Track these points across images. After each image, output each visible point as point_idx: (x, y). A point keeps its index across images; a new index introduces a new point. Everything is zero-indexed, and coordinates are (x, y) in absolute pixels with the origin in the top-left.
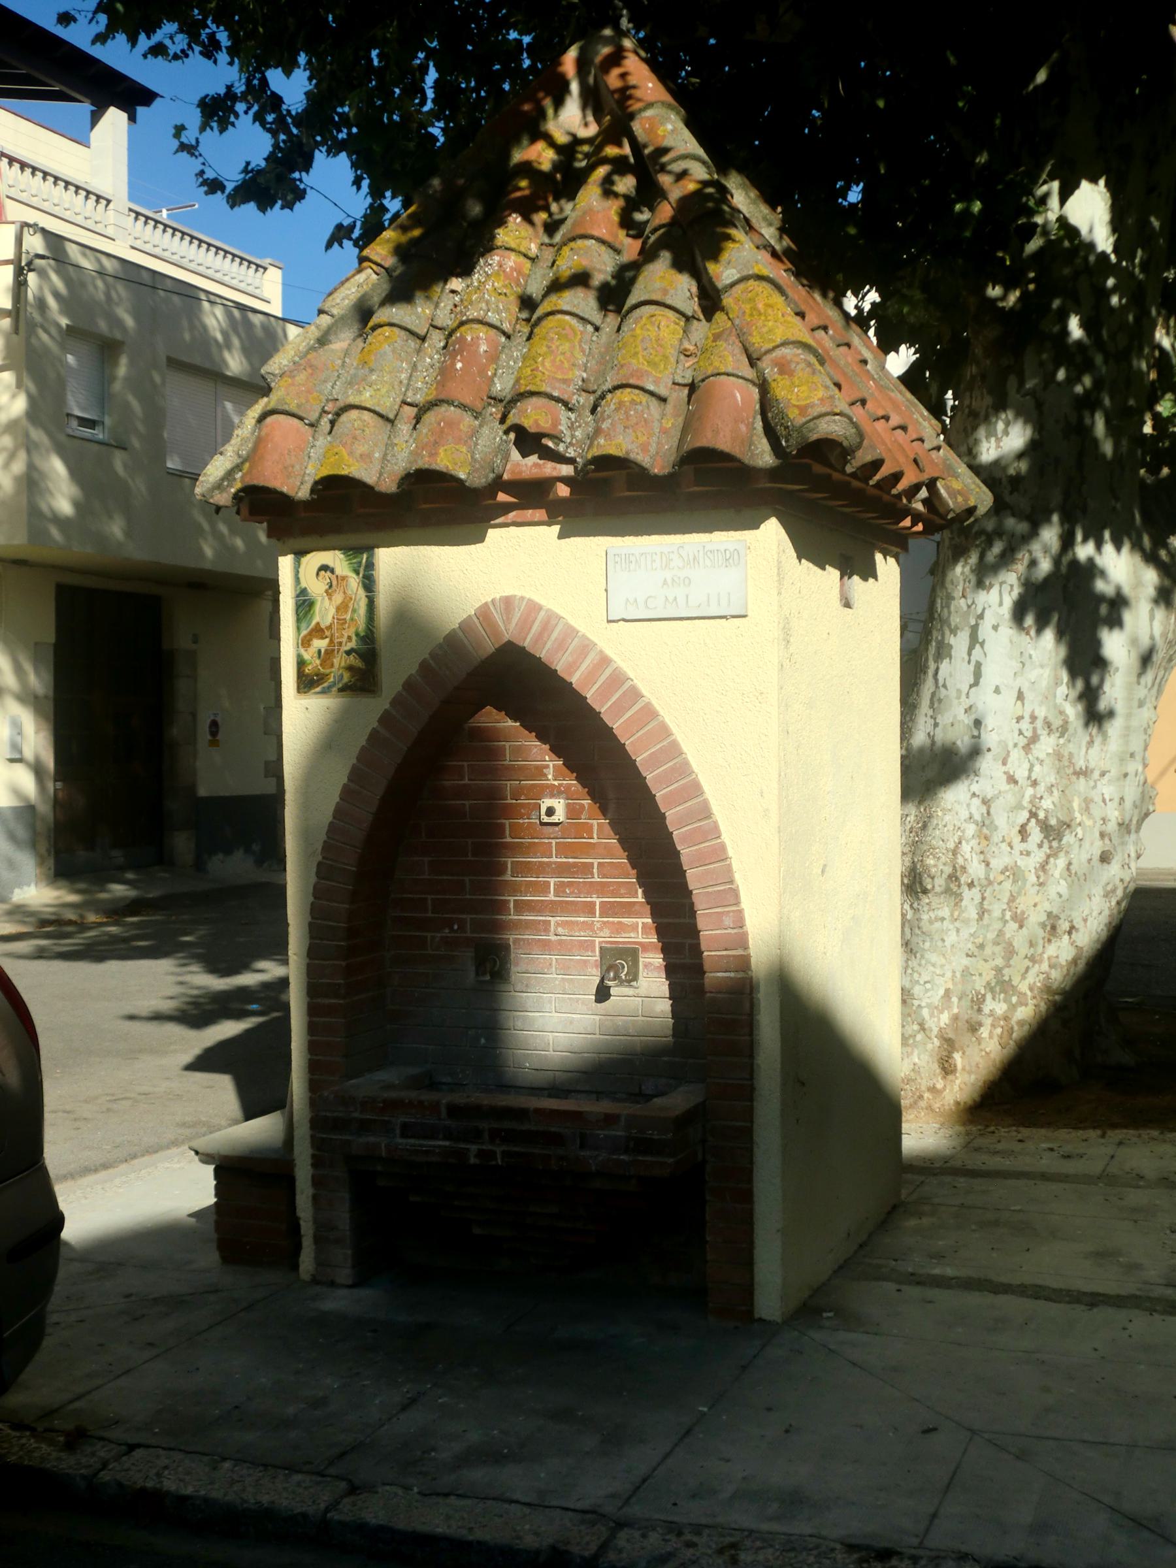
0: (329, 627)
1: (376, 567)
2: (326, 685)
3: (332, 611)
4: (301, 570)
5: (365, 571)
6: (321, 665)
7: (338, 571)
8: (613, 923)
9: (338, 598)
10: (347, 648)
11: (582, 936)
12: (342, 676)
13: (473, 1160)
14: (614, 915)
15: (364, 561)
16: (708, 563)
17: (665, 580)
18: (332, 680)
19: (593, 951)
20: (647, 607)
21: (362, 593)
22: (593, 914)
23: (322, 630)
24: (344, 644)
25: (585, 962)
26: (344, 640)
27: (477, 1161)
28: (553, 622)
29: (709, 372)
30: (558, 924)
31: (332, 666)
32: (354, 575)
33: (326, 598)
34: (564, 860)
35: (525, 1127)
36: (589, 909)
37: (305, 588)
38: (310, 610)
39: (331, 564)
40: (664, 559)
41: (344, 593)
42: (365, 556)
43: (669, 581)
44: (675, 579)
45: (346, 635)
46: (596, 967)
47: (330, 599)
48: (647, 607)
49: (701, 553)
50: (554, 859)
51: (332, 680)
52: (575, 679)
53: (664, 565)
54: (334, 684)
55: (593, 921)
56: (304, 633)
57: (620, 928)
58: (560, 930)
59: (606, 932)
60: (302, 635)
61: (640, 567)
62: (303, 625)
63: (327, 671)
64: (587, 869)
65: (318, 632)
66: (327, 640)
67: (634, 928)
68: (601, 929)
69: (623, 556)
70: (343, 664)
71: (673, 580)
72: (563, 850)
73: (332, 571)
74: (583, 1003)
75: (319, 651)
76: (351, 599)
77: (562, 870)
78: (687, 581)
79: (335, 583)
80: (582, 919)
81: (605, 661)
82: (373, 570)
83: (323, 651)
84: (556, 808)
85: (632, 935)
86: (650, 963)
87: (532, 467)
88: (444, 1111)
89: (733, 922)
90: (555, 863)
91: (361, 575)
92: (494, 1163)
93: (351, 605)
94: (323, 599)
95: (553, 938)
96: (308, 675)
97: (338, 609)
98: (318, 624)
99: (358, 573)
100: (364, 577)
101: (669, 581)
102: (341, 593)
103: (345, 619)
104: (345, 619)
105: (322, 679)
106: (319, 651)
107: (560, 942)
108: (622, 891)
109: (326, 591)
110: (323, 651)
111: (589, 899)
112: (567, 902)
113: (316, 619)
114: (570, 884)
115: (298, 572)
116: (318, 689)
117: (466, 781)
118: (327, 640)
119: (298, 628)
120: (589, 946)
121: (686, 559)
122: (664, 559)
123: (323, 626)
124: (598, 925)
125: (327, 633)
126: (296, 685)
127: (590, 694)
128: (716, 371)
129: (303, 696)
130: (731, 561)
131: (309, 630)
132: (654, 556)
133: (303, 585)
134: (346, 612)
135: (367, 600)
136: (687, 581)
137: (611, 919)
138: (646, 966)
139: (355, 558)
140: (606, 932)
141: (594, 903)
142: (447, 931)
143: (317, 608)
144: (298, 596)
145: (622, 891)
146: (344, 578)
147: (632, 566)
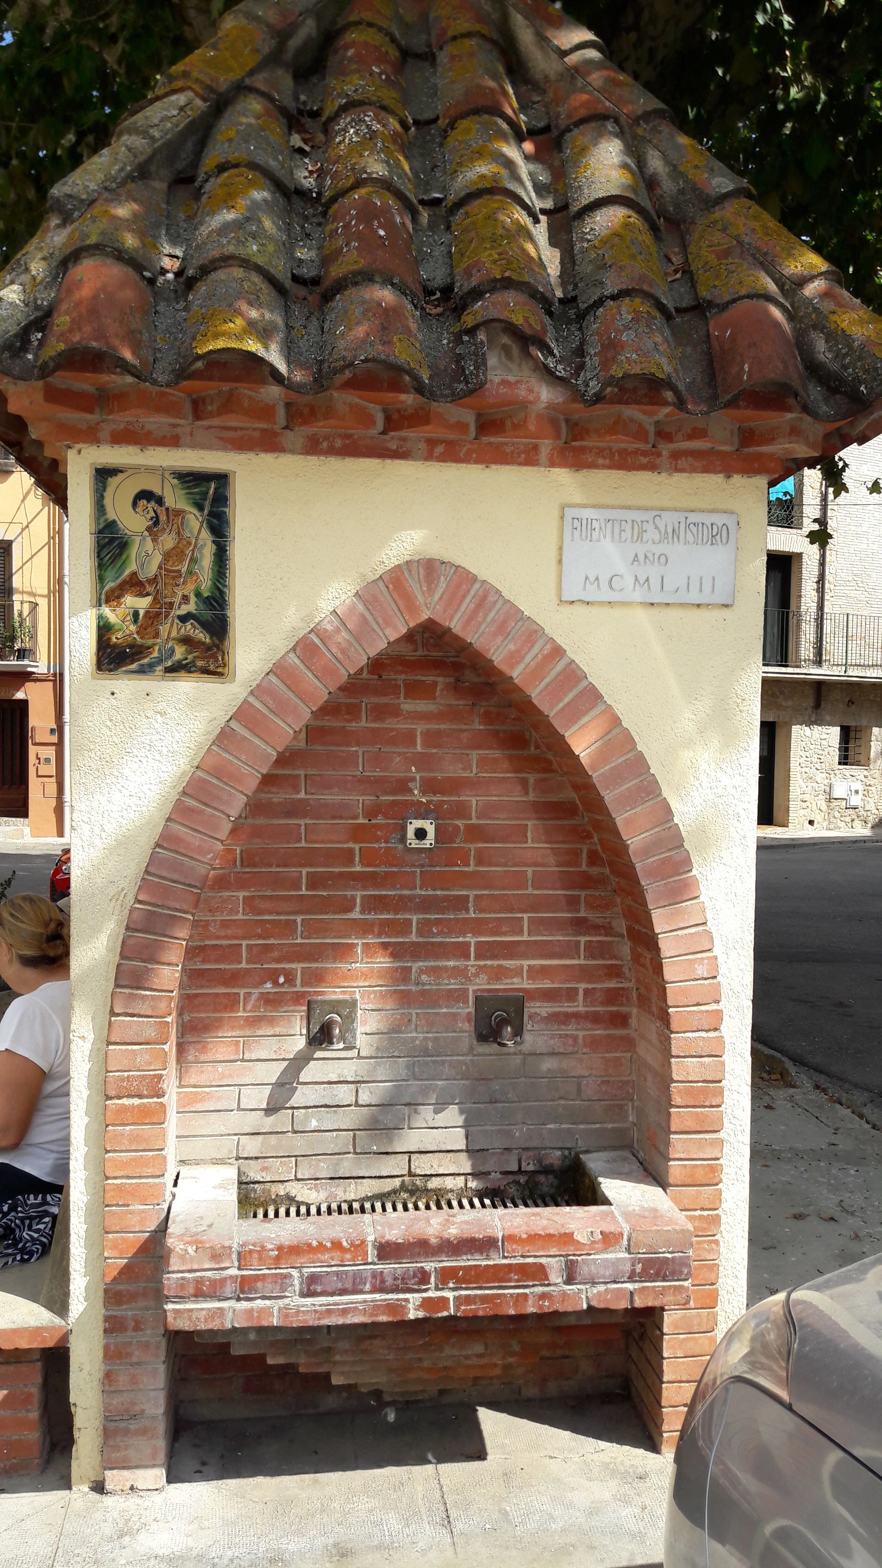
0: (154, 581)
1: (231, 502)
2: (146, 661)
3: (157, 559)
4: (108, 495)
5: (212, 506)
6: (138, 633)
7: (169, 502)
8: (492, 967)
9: (168, 541)
10: (184, 610)
11: (453, 984)
12: (172, 651)
13: (412, 1315)
14: (494, 957)
15: (211, 491)
16: (690, 538)
17: (636, 556)
18: (156, 654)
19: (466, 1002)
20: (611, 587)
21: (206, 536)
22: (468, 957)
23: (140, 584)
24: (176, 605)
25: (454, 1015)
26: (177, 600)
27: (421, 1314)
28: (491, 598)
29: (743, 292)
30: (421, 971)
31: (157, 635)
32: (195, 511)
33: (149, 539)
34: (431, 893)
35: (496, 1260)
36: (462, 951)
37: (114, 522)
38: (121, 554)
39: (157, 491)
40: (636, 531)
41: (179, 533)
42: (213, 485)
43: (641, 557)
44: (650, 555)
45: (180, 594)
46: (469, 1021)
47: (155, 540)
48: (611, 587)
49: (683, 526)
50: (418, 892)
51: (156, 654)
52: (516, 674)
53: (635, 538)
54: (160, 661)
55: (467, 966)
56: (110, 585)
57: (499, 974)
58: (424, 978)
59: (483, 978)
60: (106, 588)
61: (605, 537)
62: (110, 574)
63: (150, 642)
64: (461, 903)
65: (135, 585)
66: (149, 599)
67: (518, 972)
68: (476, 975)
69: (584, 522)
70: (174, 634)
71: (646, 557)
72: (429, 880)
73: (160, 501)
74: (450, 1066)
75: (136, 614)
76: (190, 544)
77: (426, 904)
78: (663, 559)
79: (163, 518)
80: (451, 963)
81: (558, 652)
82: (226, 505)
83: (142, 613)
84: (427, 830)
85: (515, 980)
86: (536, 1013)
87: (499, 384)
88: (372, 1254)
89: (708, 970)
90: (420, 896)
91: (206, 512)
92: (445, 1314)
93: (189, 552)
94: (144, 538)
95: (413, 988)
96: (115, 646)
97: (167, 556)
98: (134, 574)
99: (201, 508)
100: (210, 514)
101: (641, 557)
102: (173, 535)
103: (179, 571)
104: (179, 571)
105: (141, 653)
106: (136, 614)
107: (423, 992)
108: (504, 929)
109: (149, 529)
110: (142, 613)
111: (461, 939)
112: (433, 943)
113: (132, 567)
114: (438, 922)
115: (102, 497)
116: (134, 666)
117: (302, 795)
118: (149, 599)
119: (101, 579)
120: (459, 996)
121: (663, 532)
122: (636, 531)
123: (142, 577)
124: (473, 970)
125: (149, 589)
126: (94, 658)
127: (535, 693)
128: (752, 292)
129: (106, 675)
130: (718, 537)
131: (119, 581)
132: (623, 523)
133: (111, 515)
134: (181, 561)
135: (214, 547)
136: (663, 559)
137: (489, 963)
138: (530, 1017)
139: (197, 486)
140: (483, 978)
141: (468, 944)
142: (269, 985)
143: (133, 551)
144: (100, 532)
145: (504, 929)
146: (179, 513)
147: (595, 534)
